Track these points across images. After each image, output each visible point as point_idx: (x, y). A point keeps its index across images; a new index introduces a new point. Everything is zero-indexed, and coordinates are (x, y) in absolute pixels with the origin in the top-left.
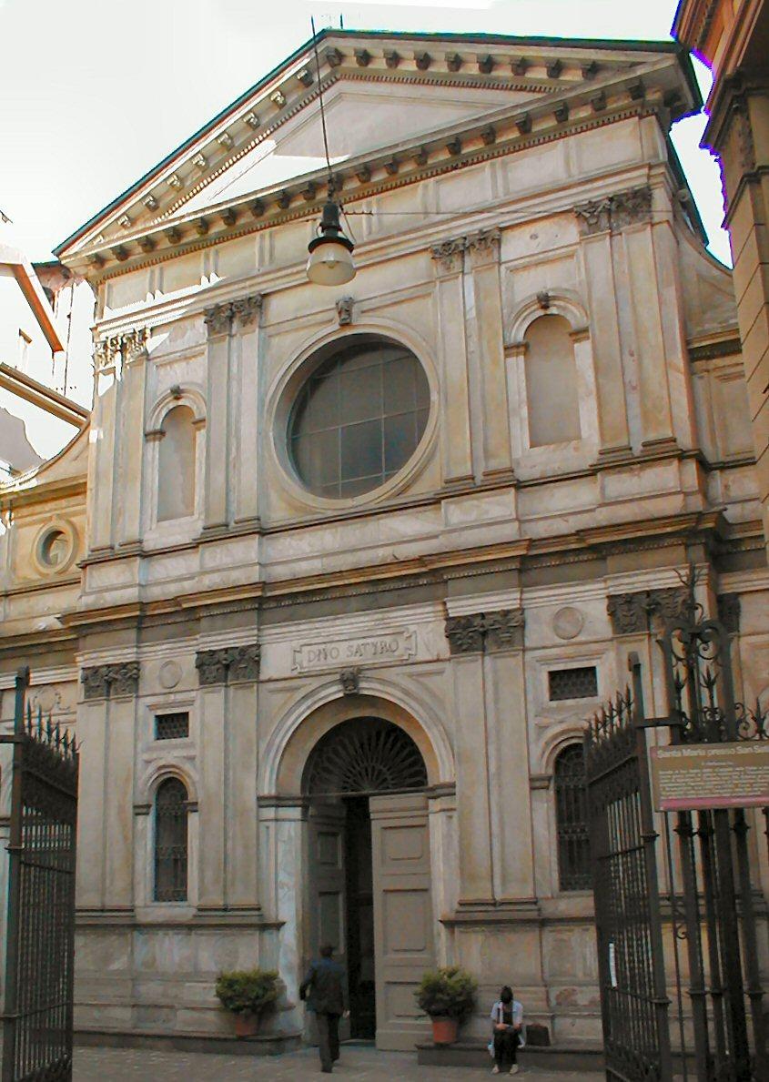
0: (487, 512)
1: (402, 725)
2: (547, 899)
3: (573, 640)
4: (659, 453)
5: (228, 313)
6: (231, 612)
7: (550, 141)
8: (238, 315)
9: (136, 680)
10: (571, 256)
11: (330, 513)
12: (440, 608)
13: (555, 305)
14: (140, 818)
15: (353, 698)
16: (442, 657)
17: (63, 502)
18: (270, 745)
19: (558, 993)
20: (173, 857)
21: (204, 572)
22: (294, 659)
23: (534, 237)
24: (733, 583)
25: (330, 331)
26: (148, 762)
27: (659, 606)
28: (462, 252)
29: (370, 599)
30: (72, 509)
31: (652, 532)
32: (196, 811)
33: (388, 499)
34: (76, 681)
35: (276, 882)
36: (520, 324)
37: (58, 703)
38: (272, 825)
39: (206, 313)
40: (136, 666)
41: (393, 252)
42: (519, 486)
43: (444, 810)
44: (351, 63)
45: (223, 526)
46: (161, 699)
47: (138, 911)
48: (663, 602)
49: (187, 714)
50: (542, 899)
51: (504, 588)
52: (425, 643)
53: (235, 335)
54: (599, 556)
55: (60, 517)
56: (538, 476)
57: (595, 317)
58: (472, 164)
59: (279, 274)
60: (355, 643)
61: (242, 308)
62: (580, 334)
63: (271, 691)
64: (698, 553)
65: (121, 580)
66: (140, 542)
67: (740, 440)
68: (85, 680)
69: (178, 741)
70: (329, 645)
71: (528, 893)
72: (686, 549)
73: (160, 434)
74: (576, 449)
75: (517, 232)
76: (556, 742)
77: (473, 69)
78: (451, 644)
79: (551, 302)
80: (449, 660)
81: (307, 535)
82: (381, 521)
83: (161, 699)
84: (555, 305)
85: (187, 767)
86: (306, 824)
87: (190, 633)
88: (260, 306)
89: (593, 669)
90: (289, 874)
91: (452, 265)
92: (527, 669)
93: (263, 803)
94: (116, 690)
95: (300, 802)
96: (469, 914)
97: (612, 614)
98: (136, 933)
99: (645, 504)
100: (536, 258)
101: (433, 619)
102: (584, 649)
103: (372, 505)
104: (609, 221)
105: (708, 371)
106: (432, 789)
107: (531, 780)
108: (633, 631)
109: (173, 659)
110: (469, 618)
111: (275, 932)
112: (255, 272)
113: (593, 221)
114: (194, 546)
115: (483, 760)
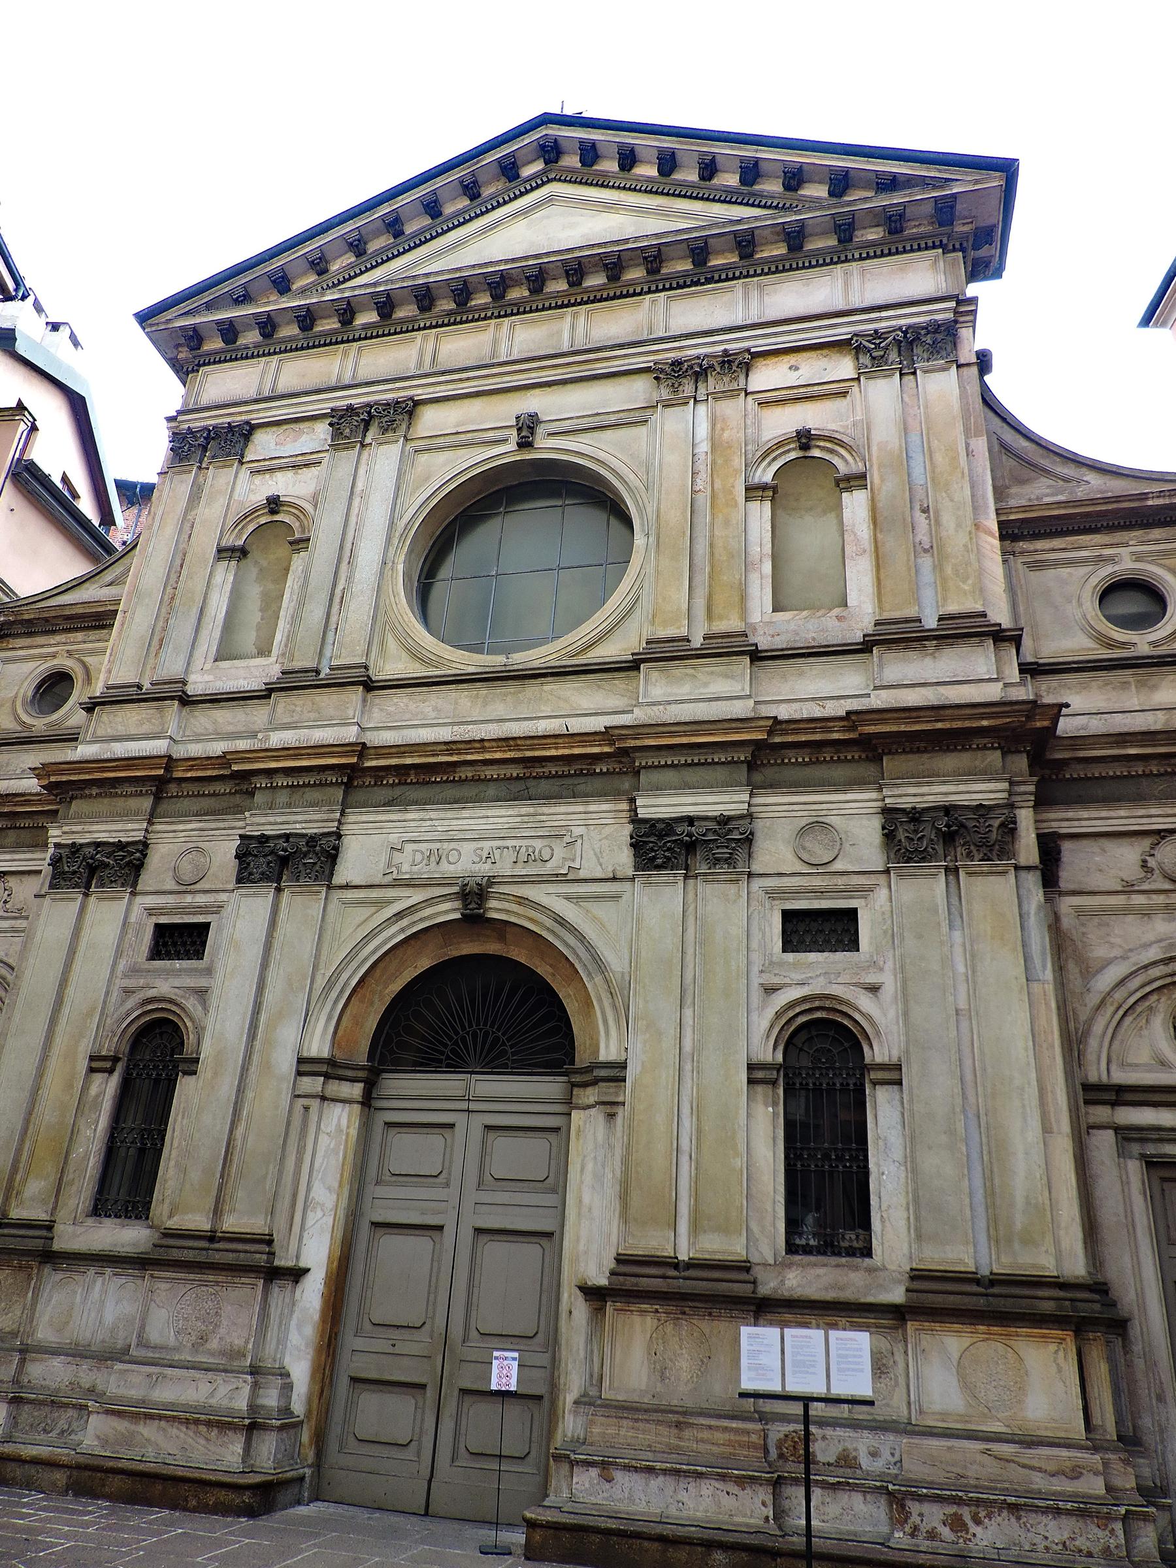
0: (706, 685)
1: (543, 970)
2: (766, 1265)
5: (365, 416)
7: (825, 264)
10: (844, 394)
11: (471, 670)
12: (625, 806)
13: (818, 447)
14: (98, 1078)
17: (80, 636)
19: (782, 1436)
22: (391, 859)
25: (507, 451)
26: (128, 992)
27: (962, 830)
28: (697, 374)
29: (520, 785)
30: (90, 645)
32: (195, 1073)
34: (40, 872)
35: (307, 1197)
36: (769, 464)
37: (5, 902)
38: (315, 1104)
40: (141, 847)
42: (757, 656)
43: (604, 1103)
44: (572, 161)
45: (312, 671)
46: (170, 900)
47: (59, 1228)
48: (971, 824)
49: (206, 926)
52: (595, 854)
54: (870, 755)
55: (70, 653)
58: (717, 282)
59: (442, 378)
60: (487, 845)
61: (386, 413)
62: (857, 480)
64: (1021, 763)
65: (146, 728)
66: (184, 683)
68: (55, 862)
69: (186, 964)
70: (445, 845)
71: (734, 1248)
72: (1004, 754)
73: (240, 553)
75: (771, 361)
76: (791, 1014)
79: (813, 443)
80: (633, 879)
81: (433, 696)
82: (546, 688)
83: (170, 900)
84: (818, 447)
85: (191, 1004)
87: (239, 810)
88: (411, 414)
89: (852, 914)
90: (329, 1189)
91: (681, 388)
92: (754, 903)
94: (101, 878)
95: (362, 1074)
96: (633, 1279)
97: (889, 836)
98: (47, 1269)
99: (941, 689)
100: (796, 391)
101: (612, 821)
102: (841, 881)
103: (536, 664)
104: (900, 355)
106: (581, 1071)
107: (751, 1067)
108: (923, 860)
109: (200, 845)
110: (669, 824)
111: (289, 1285)
115: (672, 1031)
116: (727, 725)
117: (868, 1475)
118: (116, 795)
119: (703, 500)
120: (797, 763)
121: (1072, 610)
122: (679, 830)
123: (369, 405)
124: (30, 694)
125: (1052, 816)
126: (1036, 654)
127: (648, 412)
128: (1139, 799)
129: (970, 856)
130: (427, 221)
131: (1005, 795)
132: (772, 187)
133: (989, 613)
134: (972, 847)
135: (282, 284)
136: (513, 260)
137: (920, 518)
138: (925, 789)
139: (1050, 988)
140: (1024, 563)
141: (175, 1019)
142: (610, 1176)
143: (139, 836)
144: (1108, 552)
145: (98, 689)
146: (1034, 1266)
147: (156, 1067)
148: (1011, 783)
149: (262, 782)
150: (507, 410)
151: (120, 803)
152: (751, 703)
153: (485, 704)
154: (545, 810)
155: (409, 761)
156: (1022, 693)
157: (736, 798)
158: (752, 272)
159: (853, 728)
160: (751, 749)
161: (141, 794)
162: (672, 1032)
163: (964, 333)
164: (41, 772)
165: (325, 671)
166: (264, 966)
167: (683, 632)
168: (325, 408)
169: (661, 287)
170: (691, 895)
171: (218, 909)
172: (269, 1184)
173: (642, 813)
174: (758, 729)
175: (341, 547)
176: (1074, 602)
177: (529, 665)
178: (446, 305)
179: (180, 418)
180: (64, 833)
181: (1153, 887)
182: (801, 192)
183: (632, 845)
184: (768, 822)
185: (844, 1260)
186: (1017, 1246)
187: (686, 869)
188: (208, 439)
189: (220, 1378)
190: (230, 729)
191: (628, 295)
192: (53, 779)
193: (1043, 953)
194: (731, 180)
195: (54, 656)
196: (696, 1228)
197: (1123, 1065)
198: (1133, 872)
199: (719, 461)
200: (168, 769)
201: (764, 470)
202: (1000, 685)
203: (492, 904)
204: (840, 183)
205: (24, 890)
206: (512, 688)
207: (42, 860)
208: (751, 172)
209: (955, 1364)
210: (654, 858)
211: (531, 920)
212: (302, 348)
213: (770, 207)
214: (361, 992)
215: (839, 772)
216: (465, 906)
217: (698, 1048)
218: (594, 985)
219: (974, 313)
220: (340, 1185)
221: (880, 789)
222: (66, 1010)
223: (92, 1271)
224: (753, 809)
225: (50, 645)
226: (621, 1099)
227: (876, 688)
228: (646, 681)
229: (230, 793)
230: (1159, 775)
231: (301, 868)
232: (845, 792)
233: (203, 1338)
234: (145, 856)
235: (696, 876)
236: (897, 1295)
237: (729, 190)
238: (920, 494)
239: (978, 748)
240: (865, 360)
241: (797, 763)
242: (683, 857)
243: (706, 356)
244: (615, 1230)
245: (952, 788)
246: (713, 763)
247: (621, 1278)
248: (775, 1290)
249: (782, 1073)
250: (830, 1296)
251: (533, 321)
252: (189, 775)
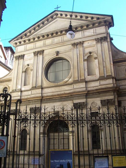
0: (80, 86)
3: (95, 107)
4: (108, 77)
10: (94, 46)
11: (53, 85)
12: (72, 101)
17: (7, 82)
21: (32, 94)
23: (88, 43)
24: (120, 99)
25: (55, 56)
31: (108, 90)
39: (34, 53)
41: (65, 44)
44: (59, 15)
56: (89, 80)
60: (57, 107)
64: (116, 93)
67: (122, 76)
73: (25, 72)
74: (95, 76)
75: (86, 42)
77: (79, 17)
81: (49, 89)
82: (62, 87)
97: (101, 103)
99: (107, 85)
103: (61, 84)
105: (116, 65)
110: (77, 104)
112: (42, 47)
113: (98, 41)
114: (30, 90)
138: (105, 97)
149: (31, 101)
153: (55, 90)
154: (63, 102)
157: (84, 100)
173: (74, 102)
178: (46, 37)
188: (19, 57)
215: (96, 96)
245: (108, 97)
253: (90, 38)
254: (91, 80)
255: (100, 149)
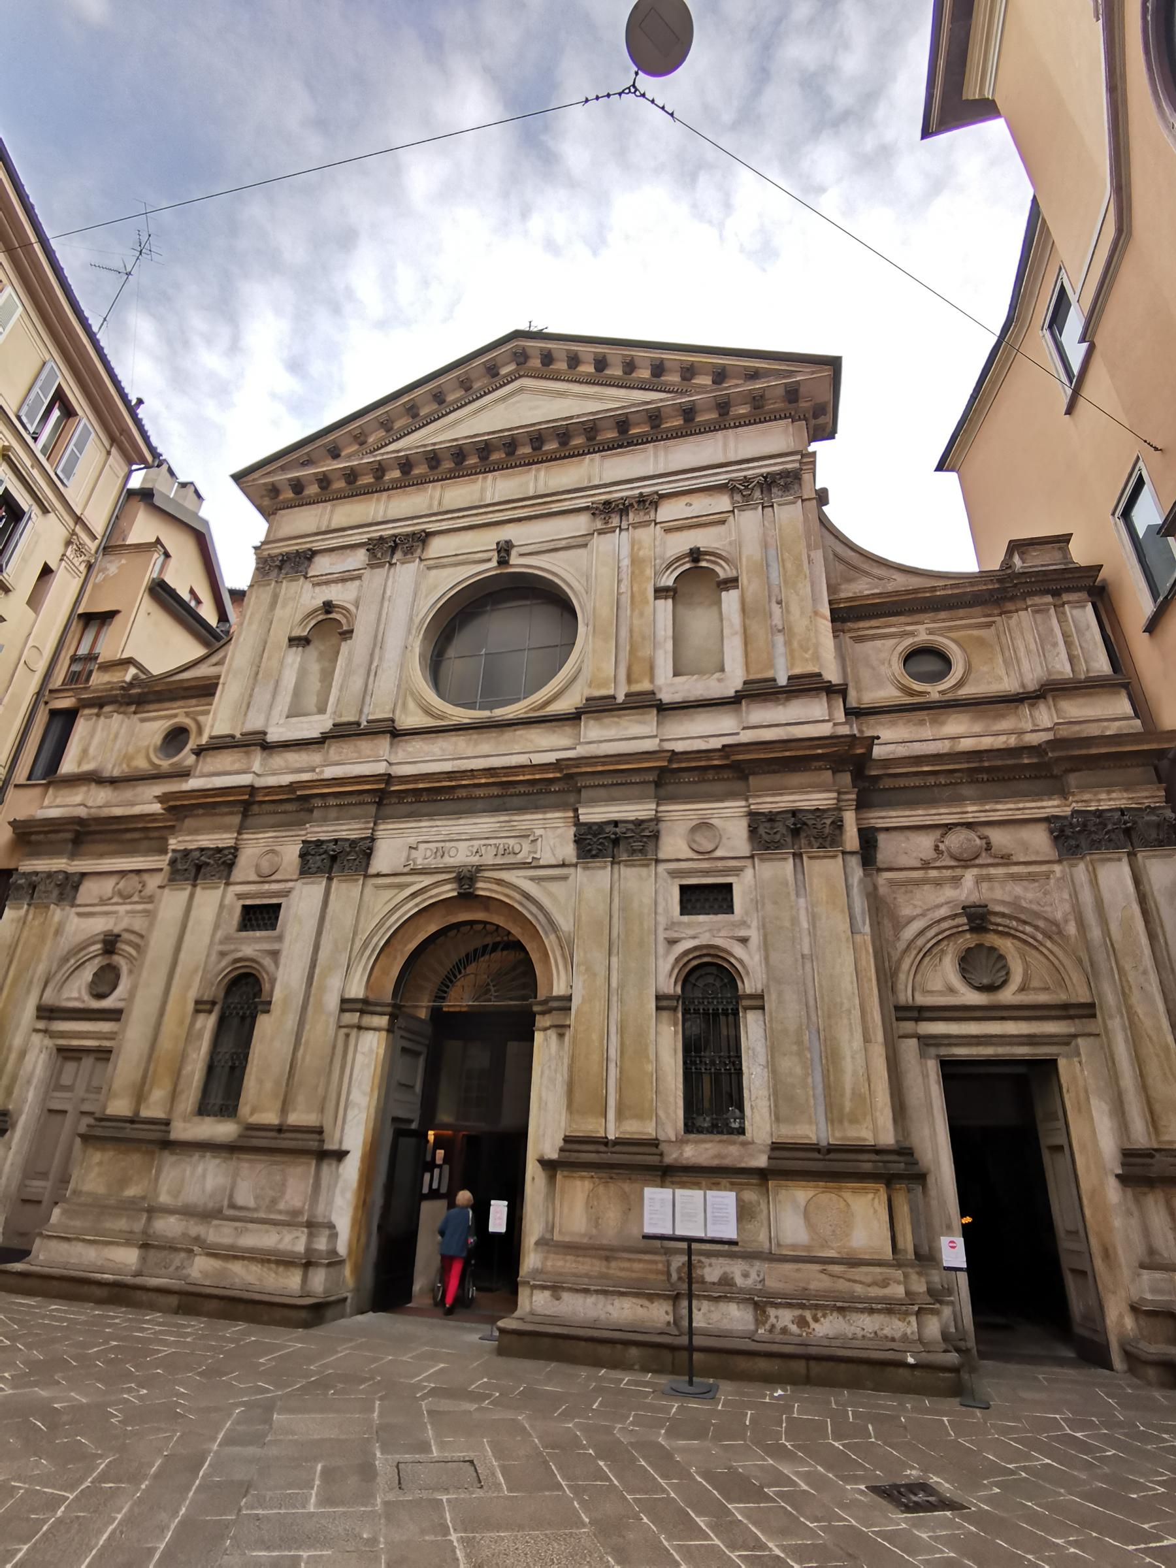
0: (626, 728)
6: (349, 804)
8: (400, 547)
9: (230, 866)
10: (723, 522)
12: (571, 814)
14: (202, 1017)
15: (467, 896)
16: (567, 863)
17: (194, 702)
18: (365, 945)
20: (230, 1064)
26: (222, 954)
27: (805, 827)
28: (621, 510)
29: (497, 802)
32: (268, 1012)
33: (526, 713)
34: (161, 870)
36: (672, 572)
37: (140, 891)
38: (354, 1032)
41: (555, 507)
44: (535, 362)
48: (810, 822)
49: (279, 906)
50: (665, 1141)
51: (640, 799)
53: (396, 564)
55: (187, 714)
57: (744, 567)
58: (636, 445)
60: (476, 843)
62: (731, 583)
63: (377, 887)
64: (846, 778)
65: (237, 766)
66: (265, 733)
68: (173, 862)
70: (448, 844)
71: (648, 1129)
72: (834, 773)
74: (720, 680)
76: (686, 959)
78: (578, 849)
79: (702, 557)
80: (575, 865)
82: (518, 733)
85: (267, 962)
86: (391, 1035)
87: (301, 824)
89: (729, 887)
92: (660, 881)
93: (346, 1006)
97: (753, 831)
98: (166, 1153)
102: (720, 864)
103: (510, 716)
104: (762, 492)
108: (777, 848)
110: (601, 825)
111: (334, 1163)
115: (603, 973)
116: (640, 757)
117: (741, 1290)
118: (216, 814)
119: (626, 600)
120: (690, 782)
121: (884, 670)
122: (607, 830)
123: (395, 536)
124: (159, 742)
125: (872, 815)
126: (859, 701)
127: (588, 538)
128: (933, 802)
129: (810, 845)
130: (435, 406)
131: (834, 801)
132: (673, 378)
133: (823, 673)
134: (812, 839)
135: (335, 454)
136: (493, 433)
137: (776, 609)
139: (868, 938)
140: (851, 638)
141: (254, 972)
142: (561, 1079)
143: (231, 843)
144: (909, 628)
145: (204, 740)
146: (859, 1139)
147: (242, 1008)
148: (839, 793)
149: (318, 802)
150: (489, 539)
151: (219, 820)
152: (657, 741)
154: (516, 818)
155: (421, 786)
156: (845, 730)
158: (659, 438)
159: (727, 757)
160: (656, 773)
161: (232, 813)
162: (603, 973)
163: (806, 477)
164: (161, 799)
165: (364, 724)
166: (319, 933)
167: (611, 692)
168: (364, 538)
169: (596, 449)
170: (616, 876)
171: (287, 893)
172: (321, 1090)
173: (583, 819)
174: (662, 759)
175: (376, 637)
176: (886, 665)
177: (506, 717)
178: (447, 465)
179: (263, 547)
180: (179, 842)
181: (944, 864)
182: (693, 381)
183: (575, 841)
184: (669, 824)
185: (725, 1137)
186: (846, 1124)
187: (613, 858)
188: (282, 561)
189: (285, 1230)
190: (297, 765)
191: (574, 456)
192: (172, 803)
193: (863, 913)
194: (645, 374)
195: (175, 716)
196: (620, 1115)
197: (926, 992)
198: (929, 854)
199: (637, 572)
200: (251, 795)
201: (668, 576)
202: (831, 724)
203: (480, 885)
204: (720, 376)
205: (153, 882)
206: (494, 734)
207: (162, 862)
208: (658, 369)
209: (802, 1209)
210: (590, 850)
211: (507, 896)
212: (349, 497)
213: (672, 392)
214: (387, 950)
215: (719, 787)
216: (461, 887)
217: (621, 986)
218: (550, 941)
219: (814, 463)
220: (372, 1090)
221: (747, 800)
222: (179, 969)
223: (196, 1156)
224: (659, 815)
225: (172, 709)
226: (568, 1023)
227: (744, 728)
228: (585, 727)
229: (297, 811)
230: (946, 785)
231: (345, 863)
232: (722, 801)
233: (274, 1201)
234: (236, 857)
235: (619, 863)
236: (761, 1161)
237: (643, 381)
238: (776, 591)
239: (816, 769)
240: (738, 497)
241: (690, 782)
242: (611, 849)
243: (627, 497)
244: (563, 1118)
246: (632, 783)
247: (567, 1154)
248: (676, 1159)
249: (680, 1002)
250: (715, 1163)
251: (509, 475)
252: (267, 799)
253: (703, 480)
254: (692, 699)
255: (742, 1138)
